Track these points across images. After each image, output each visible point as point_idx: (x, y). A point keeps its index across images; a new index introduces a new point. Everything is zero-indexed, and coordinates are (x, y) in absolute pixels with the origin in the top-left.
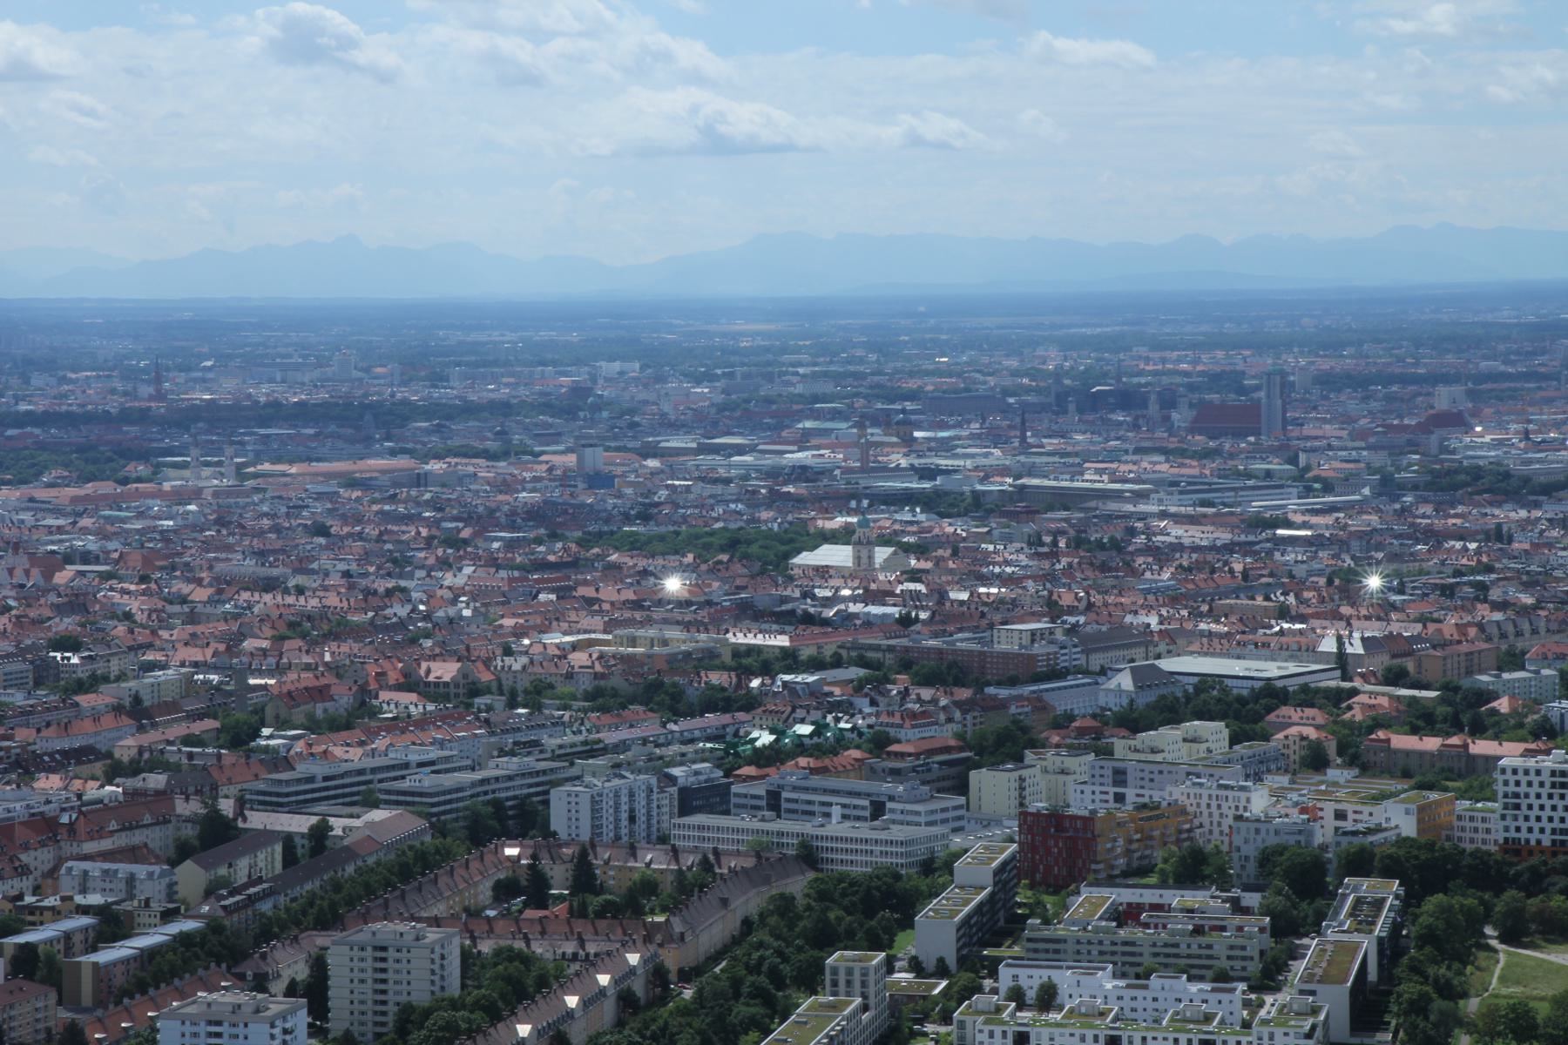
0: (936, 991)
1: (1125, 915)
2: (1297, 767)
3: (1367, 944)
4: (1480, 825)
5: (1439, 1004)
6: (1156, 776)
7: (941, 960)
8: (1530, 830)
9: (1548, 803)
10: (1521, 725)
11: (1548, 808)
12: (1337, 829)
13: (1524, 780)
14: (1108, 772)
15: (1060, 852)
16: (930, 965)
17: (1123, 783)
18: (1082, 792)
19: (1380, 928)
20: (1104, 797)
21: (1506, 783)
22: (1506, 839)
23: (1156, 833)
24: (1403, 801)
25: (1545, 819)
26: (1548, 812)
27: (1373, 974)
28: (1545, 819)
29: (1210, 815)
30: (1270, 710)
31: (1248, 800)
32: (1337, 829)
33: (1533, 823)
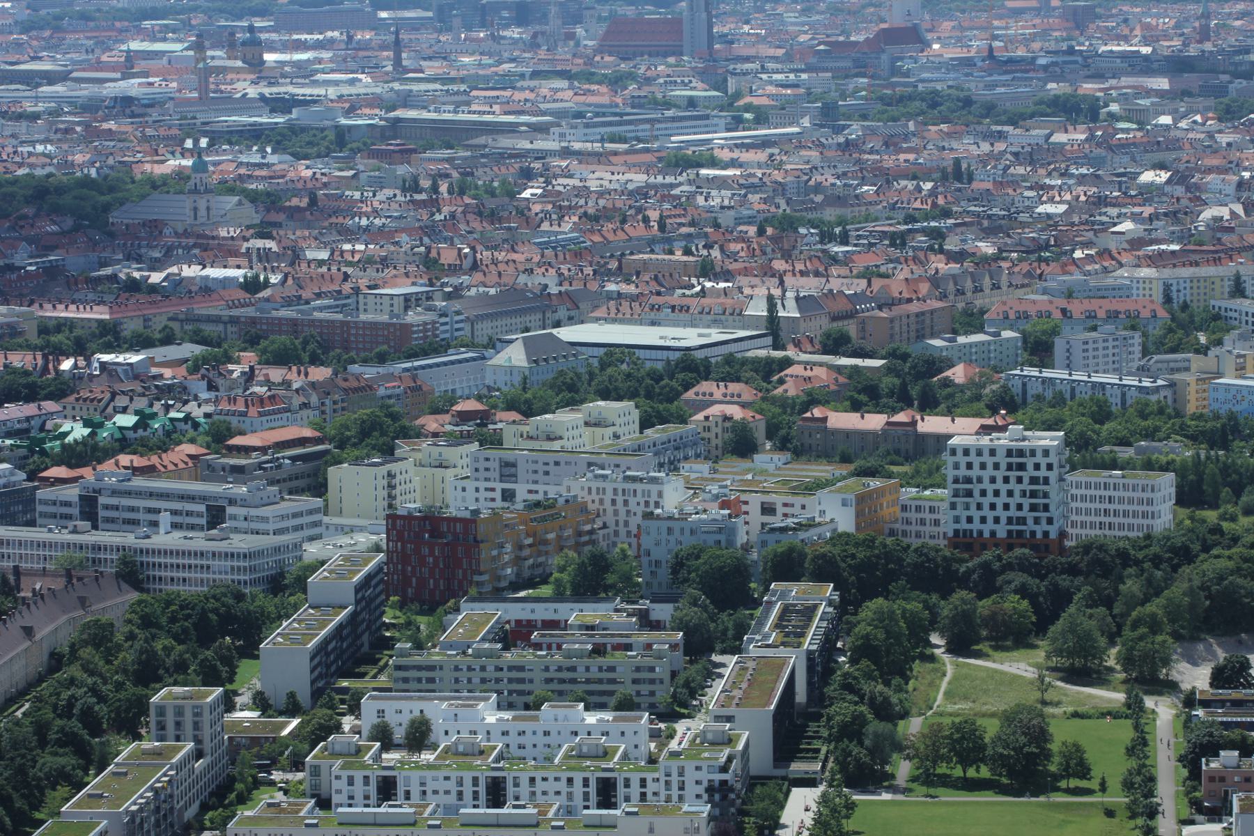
0: (286, 732)
1: (513, 635)
2: (719, 452)
3: (794, 659)
4: (927, 516)
5: (875, 726)
6: (551, 468)
7: (292, 696)
8: (983, 520)
9: (1003, 488)
10: (978, 398)
11: (1003, 493)
12: (763, 525)
13: (976, 462)
14: (494, 465)
15: (436, 560)
16: (280, 701)
17: (513, 477)
18: (464, 489)
19: (810, 641)
21: (956, 466)
22: (956, 532)
24: (839, 491)
25: (1000, 507)
26: (1003, 498)
27: (801, 695)
28: (1000, 507)
29: (616, 513)
30: (687, 387)
31: (660, 494)
32: (763, 525)
33: (986, 511)
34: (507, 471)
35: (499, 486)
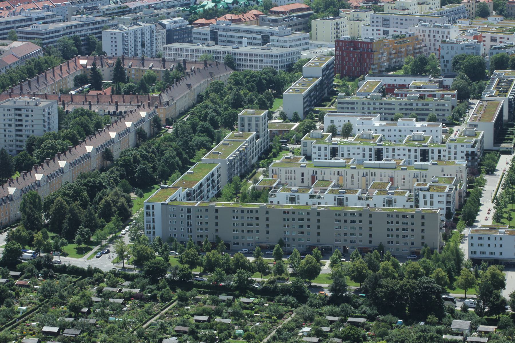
0: (293, 129)
1: (387, 90)
2: (474, 16)
3: (503, 102)
6: (404, 22)
7: (296, 114)
12: (491, 46)
14: (380, 20)
15: (355, 59)
16: (292, 116)
18: (367, 30)
20: (379, 32)
23: (403, 50)
27: (506, 117)
29: (430, 40)
31: (449, 33)
32: (491, 46)
34: (386, 22)
35: (382, 29)
